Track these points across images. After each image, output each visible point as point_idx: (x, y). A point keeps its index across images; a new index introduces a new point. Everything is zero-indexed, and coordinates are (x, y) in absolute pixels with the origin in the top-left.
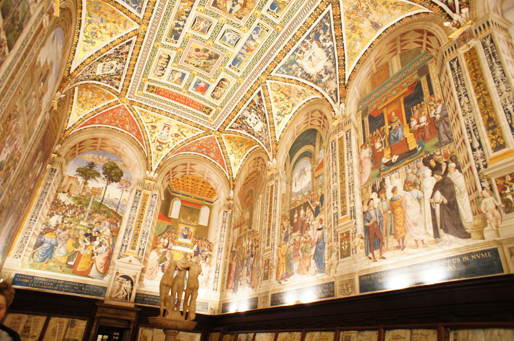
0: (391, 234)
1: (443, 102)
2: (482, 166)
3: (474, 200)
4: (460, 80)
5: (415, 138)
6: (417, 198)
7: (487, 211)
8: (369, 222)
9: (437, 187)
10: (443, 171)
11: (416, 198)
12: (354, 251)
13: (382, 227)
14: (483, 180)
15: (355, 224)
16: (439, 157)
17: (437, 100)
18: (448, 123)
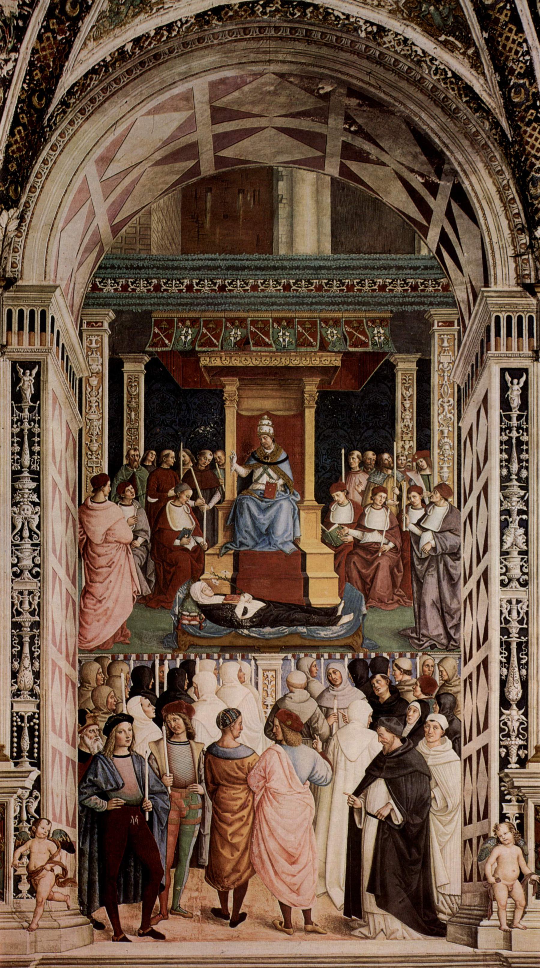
0: (195, 862)
1: (453, 500)
2: (514, 759)
3: (475, 842)
4: (520, 461)
5: (337, 570)
6: (308, 779)
7: (498, 880)
8: (105, 795)
9: (380, 769)
10: (409, 728)
11: (305, 774)
12: (24, 887)
13: (164, 831)
14: (508, 797)
15: (38, 784)
16: (407, 677)
17: (436, 481)
18: (453, 584)
